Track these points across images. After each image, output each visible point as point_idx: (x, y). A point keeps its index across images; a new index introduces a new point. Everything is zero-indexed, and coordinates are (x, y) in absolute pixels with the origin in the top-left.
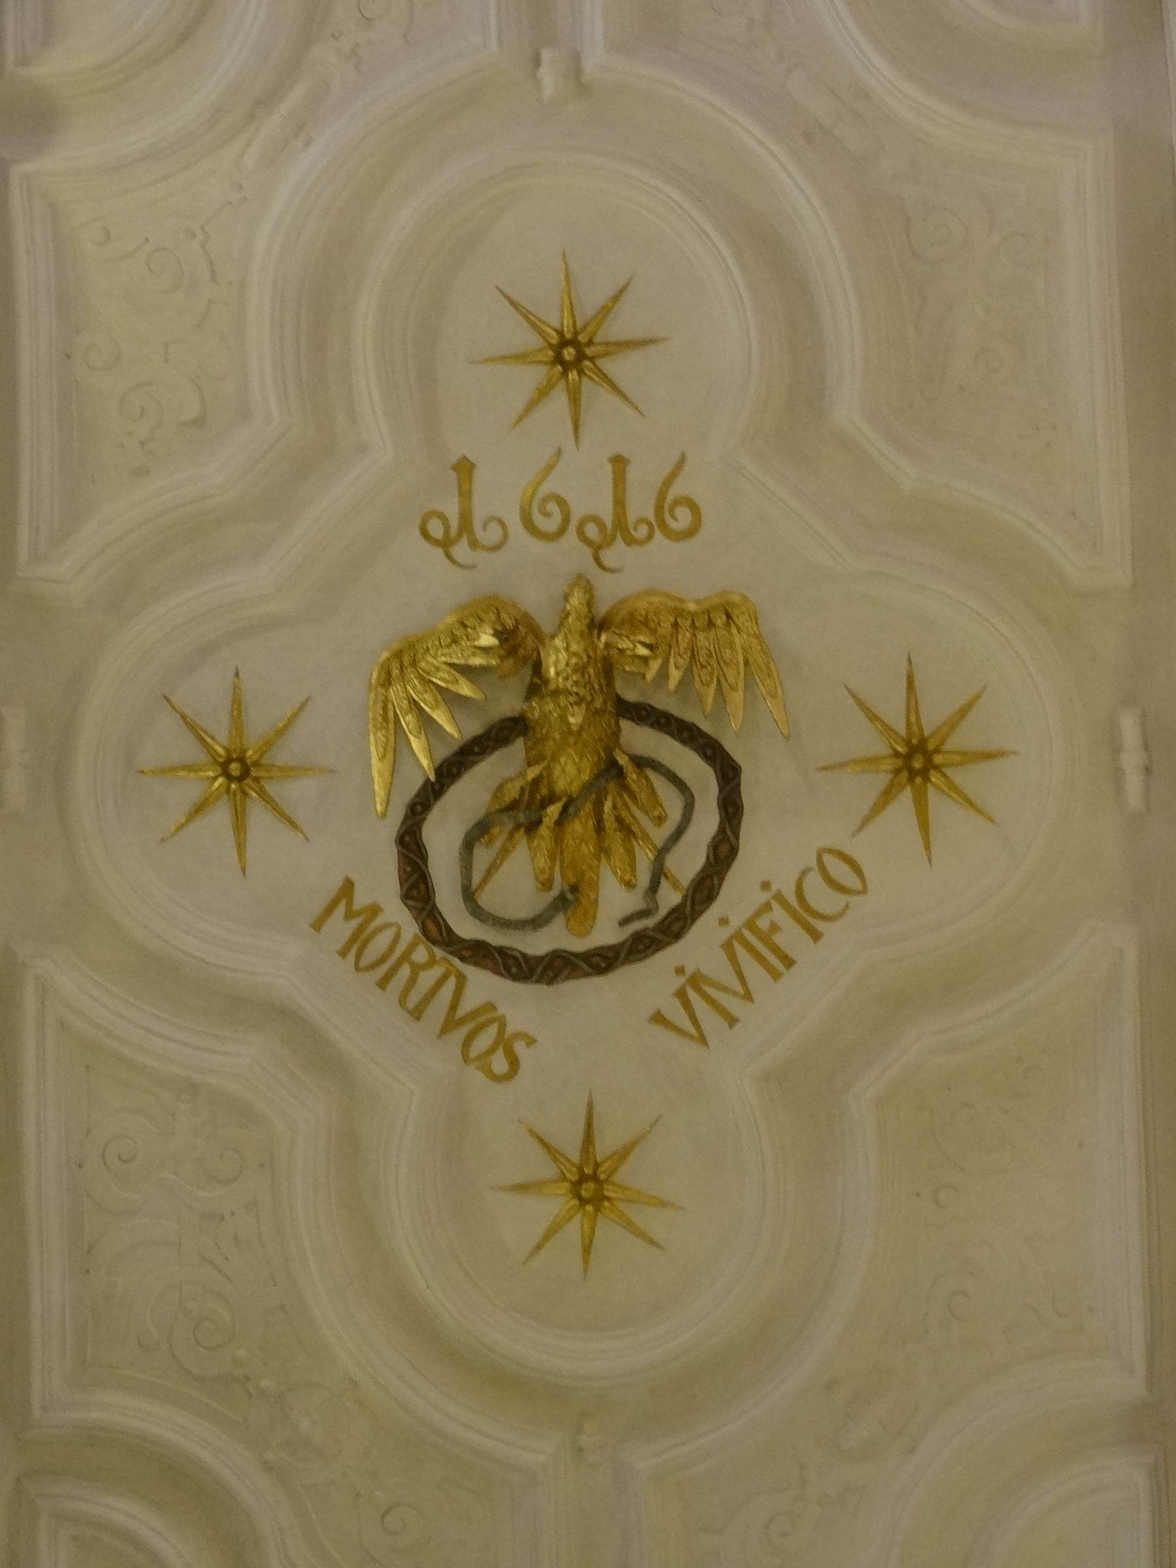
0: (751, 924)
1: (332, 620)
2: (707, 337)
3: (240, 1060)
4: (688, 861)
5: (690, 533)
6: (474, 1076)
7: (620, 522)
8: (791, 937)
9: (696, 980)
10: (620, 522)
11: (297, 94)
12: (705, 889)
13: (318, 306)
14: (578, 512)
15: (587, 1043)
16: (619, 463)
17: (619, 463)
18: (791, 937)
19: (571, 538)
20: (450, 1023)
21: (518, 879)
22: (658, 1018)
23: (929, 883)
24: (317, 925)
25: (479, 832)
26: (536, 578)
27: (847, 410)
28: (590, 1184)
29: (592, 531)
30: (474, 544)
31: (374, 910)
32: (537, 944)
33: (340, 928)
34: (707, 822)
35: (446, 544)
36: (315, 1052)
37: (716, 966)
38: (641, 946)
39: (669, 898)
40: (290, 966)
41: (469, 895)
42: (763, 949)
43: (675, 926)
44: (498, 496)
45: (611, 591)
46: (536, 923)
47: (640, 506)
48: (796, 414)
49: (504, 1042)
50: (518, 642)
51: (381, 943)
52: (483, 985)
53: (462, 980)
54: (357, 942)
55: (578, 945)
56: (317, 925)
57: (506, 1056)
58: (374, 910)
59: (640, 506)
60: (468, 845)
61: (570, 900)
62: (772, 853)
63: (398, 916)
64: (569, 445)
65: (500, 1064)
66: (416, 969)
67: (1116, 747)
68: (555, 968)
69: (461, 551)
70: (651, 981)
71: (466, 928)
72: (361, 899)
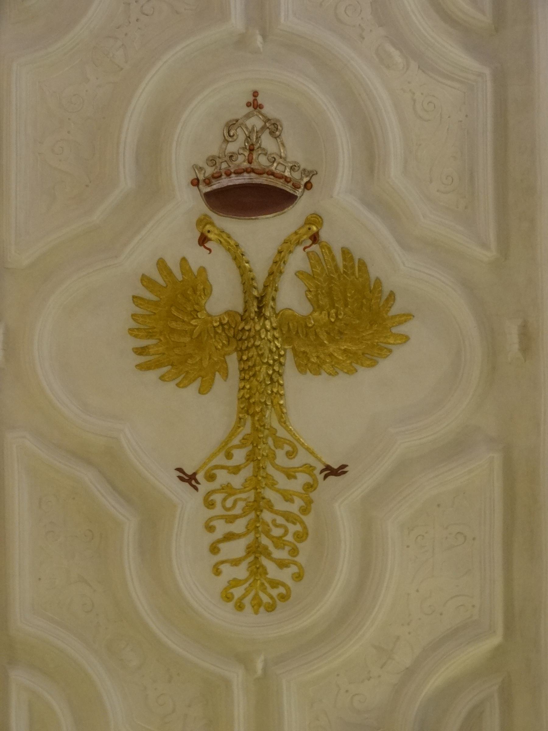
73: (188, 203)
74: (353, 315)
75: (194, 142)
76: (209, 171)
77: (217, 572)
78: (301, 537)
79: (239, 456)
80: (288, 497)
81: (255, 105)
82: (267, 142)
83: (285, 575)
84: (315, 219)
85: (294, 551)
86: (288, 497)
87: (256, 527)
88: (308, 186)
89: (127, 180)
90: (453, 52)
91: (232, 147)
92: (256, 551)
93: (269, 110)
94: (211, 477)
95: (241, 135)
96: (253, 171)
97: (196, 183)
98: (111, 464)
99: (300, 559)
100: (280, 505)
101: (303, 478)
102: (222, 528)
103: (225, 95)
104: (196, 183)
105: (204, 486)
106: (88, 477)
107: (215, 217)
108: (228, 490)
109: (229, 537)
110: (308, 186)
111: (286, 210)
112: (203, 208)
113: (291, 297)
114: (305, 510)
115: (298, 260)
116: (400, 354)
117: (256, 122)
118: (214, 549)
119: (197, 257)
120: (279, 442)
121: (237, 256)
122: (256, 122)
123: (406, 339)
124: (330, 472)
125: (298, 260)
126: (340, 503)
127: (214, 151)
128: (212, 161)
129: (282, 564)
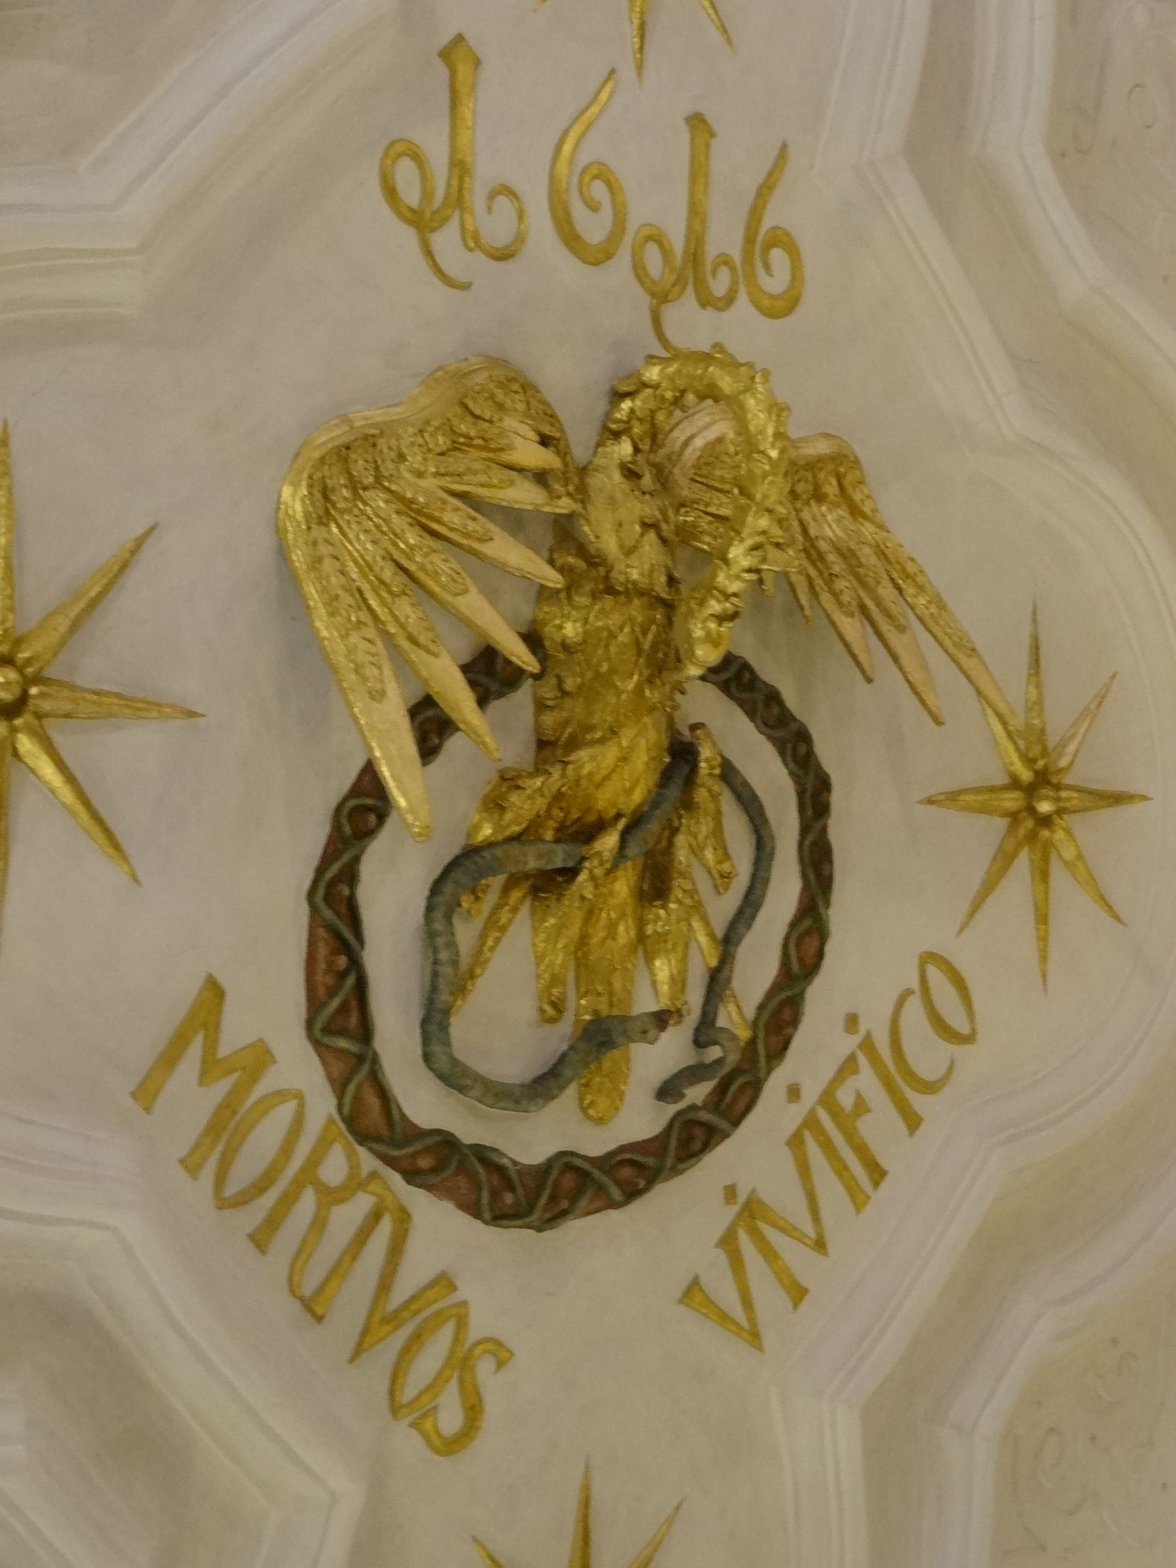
0: (828, 1099)
6: (406, 1442)
7: (694, 256)
9: (752, 1212)
10: (694, 256)
14: (638, 215)
19: (620, 269)
20: (381, 1318)
22: (693, 1292)
24: (146, 1094)
29: (653, 259)
30: (473, 241)
31: (260, 1058)
32: (531, 1139)
33: (190, 1100)
35: (423, 222)
37: (777, 1184)
41: (434, 1022)
46: (543, 1086)
51: (266, 1137)
52: (441, 1229)
53: (403, 1217)
54: (225, 1128)
55: (596, 1143)
56: (146, 1094)
58: (260, 1058)
63: (300, 1071)
64: (627, 71)
65: (450, 1419)
66: (331, 1196)
69: (447, 241)
71: (424, 1103)
72: (236, 1031)
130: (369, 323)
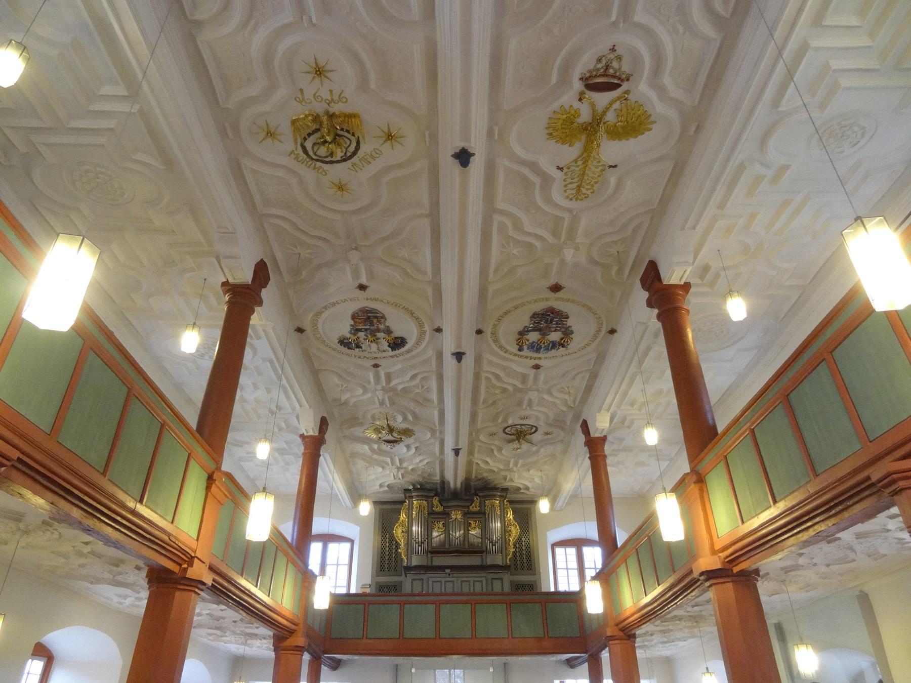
1: (283, 106)
2: (345, 76)
3: (280, 173)
4: (352, 149)
5: (346, 101)
7: (332, 100)
8: (370, 159)
11: (252, 23)
12: (355, 153)
13: (268, 61)
15: (339, 171)
16: (331, 91)
17: (331, 91)
18: (370, 159)
21: (323, 151)
23: (392, 155)
25: (314, 144)
26: (319, 108)
27: (373, 86)
28: (341, 187)
32: (327, 159)
34: (354, 144)
35: (300, 102)
36: (293, 171)
38: (345, 159)
39: (349, 154)
40: (285, 161)
41: (315, 154)
42: (365, 161)
43: (351, 157)
44: (309, 94)
45: (332, 111)
47: (336, 97)
48: (363, 83)
49: (324, 171)
50: (316, 119)
52: (319, 164)
57: (326, 173)
59: (336, 97)
60: (313, 148)
61: (331, 155)
62: (365, 149)
67: (425, 135)
68: (331, 162)
70: (348, 164)
73: (578, 86)
74: (634, 125)
75: (585, 63)
76: (588, 75)
77: (565, 191)
78: (596, 183)
79: (580, 163)
80: (594, 173)
81: (613, 50)
82: (615, 64)
83: (589, 192)
84: (627, 92)
85: (593, 186)
86: (594, 173)
87: (581, 180)
88: (628, 80)
89: (554, 80)
90: (707, 29)
91: (599, 66)
92: (579, 187)
93: (619, 51)
94: (569, 168)
95: (604, 62)
96: (607, 76)
97: (581, 79)
98: (534, 167)
99: (595, 188)
100: (590, 174)
101: (601, 168)
102: (569, 181)
103: (602, 47)
104: (581, 79)
105: (565, 170)
106: (527, 172)
107: (586, 91)
108: (573, 172)
109: (572, 183)
110: (628, 80)
111: (707, 408)
112: (583, 88)
113: (610, 117)
114: (599, 176)
115: (617, 105)
116: (647, 133)
117: (612, 56)
118: (565, 186)
119: (577, 105)
120: (595, 158)
121: (593, 105)
122: (612, 56)
123: (651, 129)
124: (610, 167)
125: (617, 105)
126: (613, 178)
127: (592, 67)
128: (590, 71)
129: (587, 189)
130: (298, 111)
